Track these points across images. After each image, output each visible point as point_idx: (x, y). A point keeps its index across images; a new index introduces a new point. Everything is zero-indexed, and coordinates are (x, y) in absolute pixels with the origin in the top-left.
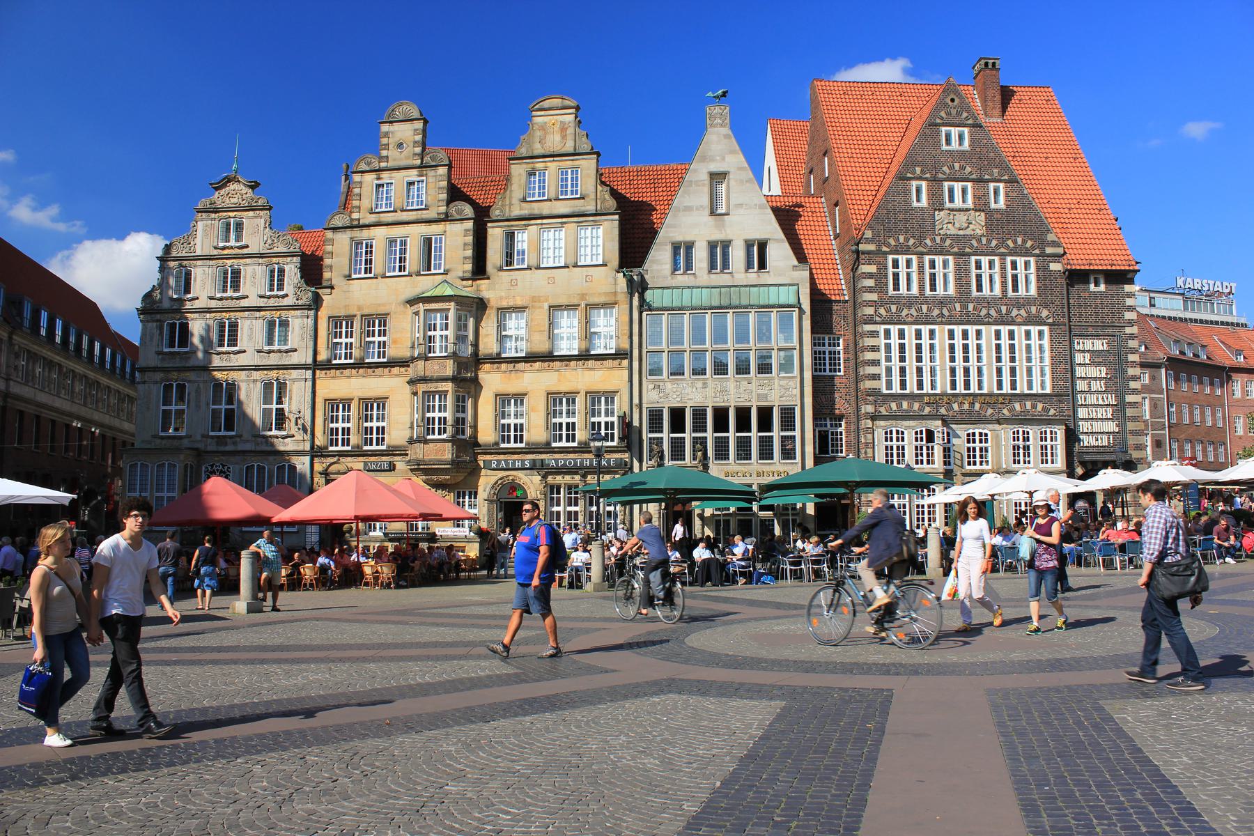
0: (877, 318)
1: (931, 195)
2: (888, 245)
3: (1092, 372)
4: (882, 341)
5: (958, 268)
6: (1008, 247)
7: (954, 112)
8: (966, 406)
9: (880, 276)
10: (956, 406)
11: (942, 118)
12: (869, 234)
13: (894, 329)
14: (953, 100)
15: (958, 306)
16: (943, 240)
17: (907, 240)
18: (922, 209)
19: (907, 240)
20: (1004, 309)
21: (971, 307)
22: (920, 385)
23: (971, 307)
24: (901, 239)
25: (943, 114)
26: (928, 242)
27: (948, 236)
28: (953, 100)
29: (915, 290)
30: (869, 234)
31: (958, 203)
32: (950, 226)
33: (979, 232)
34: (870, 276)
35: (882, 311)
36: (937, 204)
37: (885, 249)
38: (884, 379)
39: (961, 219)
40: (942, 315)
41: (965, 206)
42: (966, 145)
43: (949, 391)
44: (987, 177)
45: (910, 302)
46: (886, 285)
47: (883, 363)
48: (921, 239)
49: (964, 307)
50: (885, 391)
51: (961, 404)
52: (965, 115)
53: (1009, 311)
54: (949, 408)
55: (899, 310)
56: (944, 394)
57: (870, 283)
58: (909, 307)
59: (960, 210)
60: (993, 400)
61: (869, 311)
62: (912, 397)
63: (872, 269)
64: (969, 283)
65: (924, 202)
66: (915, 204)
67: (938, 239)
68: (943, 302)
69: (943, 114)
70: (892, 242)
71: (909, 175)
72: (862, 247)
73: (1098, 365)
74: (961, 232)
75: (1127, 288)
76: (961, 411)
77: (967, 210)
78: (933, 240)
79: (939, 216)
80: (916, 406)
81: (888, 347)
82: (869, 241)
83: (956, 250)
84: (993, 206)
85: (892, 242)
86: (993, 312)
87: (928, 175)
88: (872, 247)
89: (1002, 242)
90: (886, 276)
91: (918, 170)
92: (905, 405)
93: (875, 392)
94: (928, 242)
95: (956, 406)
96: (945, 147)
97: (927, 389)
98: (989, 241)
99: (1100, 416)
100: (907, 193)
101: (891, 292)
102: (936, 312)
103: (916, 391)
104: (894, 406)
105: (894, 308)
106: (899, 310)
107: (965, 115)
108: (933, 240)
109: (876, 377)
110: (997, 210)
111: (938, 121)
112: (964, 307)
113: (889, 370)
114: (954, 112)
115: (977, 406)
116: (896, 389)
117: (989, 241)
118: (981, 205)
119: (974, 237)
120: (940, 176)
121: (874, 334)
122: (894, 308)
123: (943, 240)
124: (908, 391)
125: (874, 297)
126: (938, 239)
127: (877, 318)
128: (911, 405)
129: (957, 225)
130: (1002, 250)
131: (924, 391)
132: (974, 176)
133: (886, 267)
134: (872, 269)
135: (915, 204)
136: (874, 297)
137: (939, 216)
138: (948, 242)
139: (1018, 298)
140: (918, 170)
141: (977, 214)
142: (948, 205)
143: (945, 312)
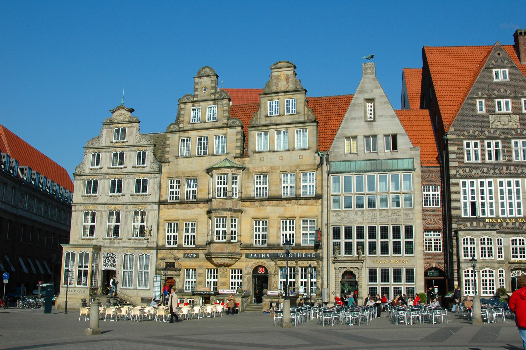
0: (458, 176)
2: (464, 135)
8: (511, 224)
9: (460, 153)
13: (468, 181)
15: (504, 168)
17: (474, 132)
19: (474, 132)
21: (512, 168)
23: (512, 168)
24: (471, 131)
26: (486, 133)
27: (498, 129)
33: (516, 126)
34: (454, 152)
35: (461, 172)
36: (491, 111)
37: (462, 137)
38: (463, 209)
39: (505, 119)
40: (495, 173)
41: (508, 112)
44: (520, 95)
45: (476, 166)
46: (463, 157)
47: (462, 201)
48: (482, 132)
49: (508, 168)
50: (463, 216)
51: (507, 223)
54: (501, 225)
55: (471, 171)
58: (476, 170)
59: (504, 114)
65: (484, 111)
66: (479, 112)
67: (492, 131)
68: (494, 166)
70: (466, 134)
74: (505, 127)
76: (508, 227)
77: (508, 114)
78: (489, 132)
79: (491, 118)
80: (481, 224)
81: (465, 192)
82: (452, 133)
83: (502, 137)
85: (466, 134)
87: (486, 96)
88: (454, 137)
90: (463, 152)
92: (475, 224)
93: (459, 216)
94: (486, 133)
101: (466, 161)
102: (492, 172)
104: (468, 224)
106: (471, 171)
108: (489, 132)
109: (458, 208)
112: (508, 168)
113: (465, 204)
119: (513, 129)
120: (493, 96)
121: (457, 185)
126: (492, 131)
127: (458, 176)
129: (502, 123)
132: (512, 95)
133: (463, 148)
135: (479, 112)
136: (456, 164)
137: (491, 118)
138: (498, 132)
141: (514, 116)
143: (497, 171)
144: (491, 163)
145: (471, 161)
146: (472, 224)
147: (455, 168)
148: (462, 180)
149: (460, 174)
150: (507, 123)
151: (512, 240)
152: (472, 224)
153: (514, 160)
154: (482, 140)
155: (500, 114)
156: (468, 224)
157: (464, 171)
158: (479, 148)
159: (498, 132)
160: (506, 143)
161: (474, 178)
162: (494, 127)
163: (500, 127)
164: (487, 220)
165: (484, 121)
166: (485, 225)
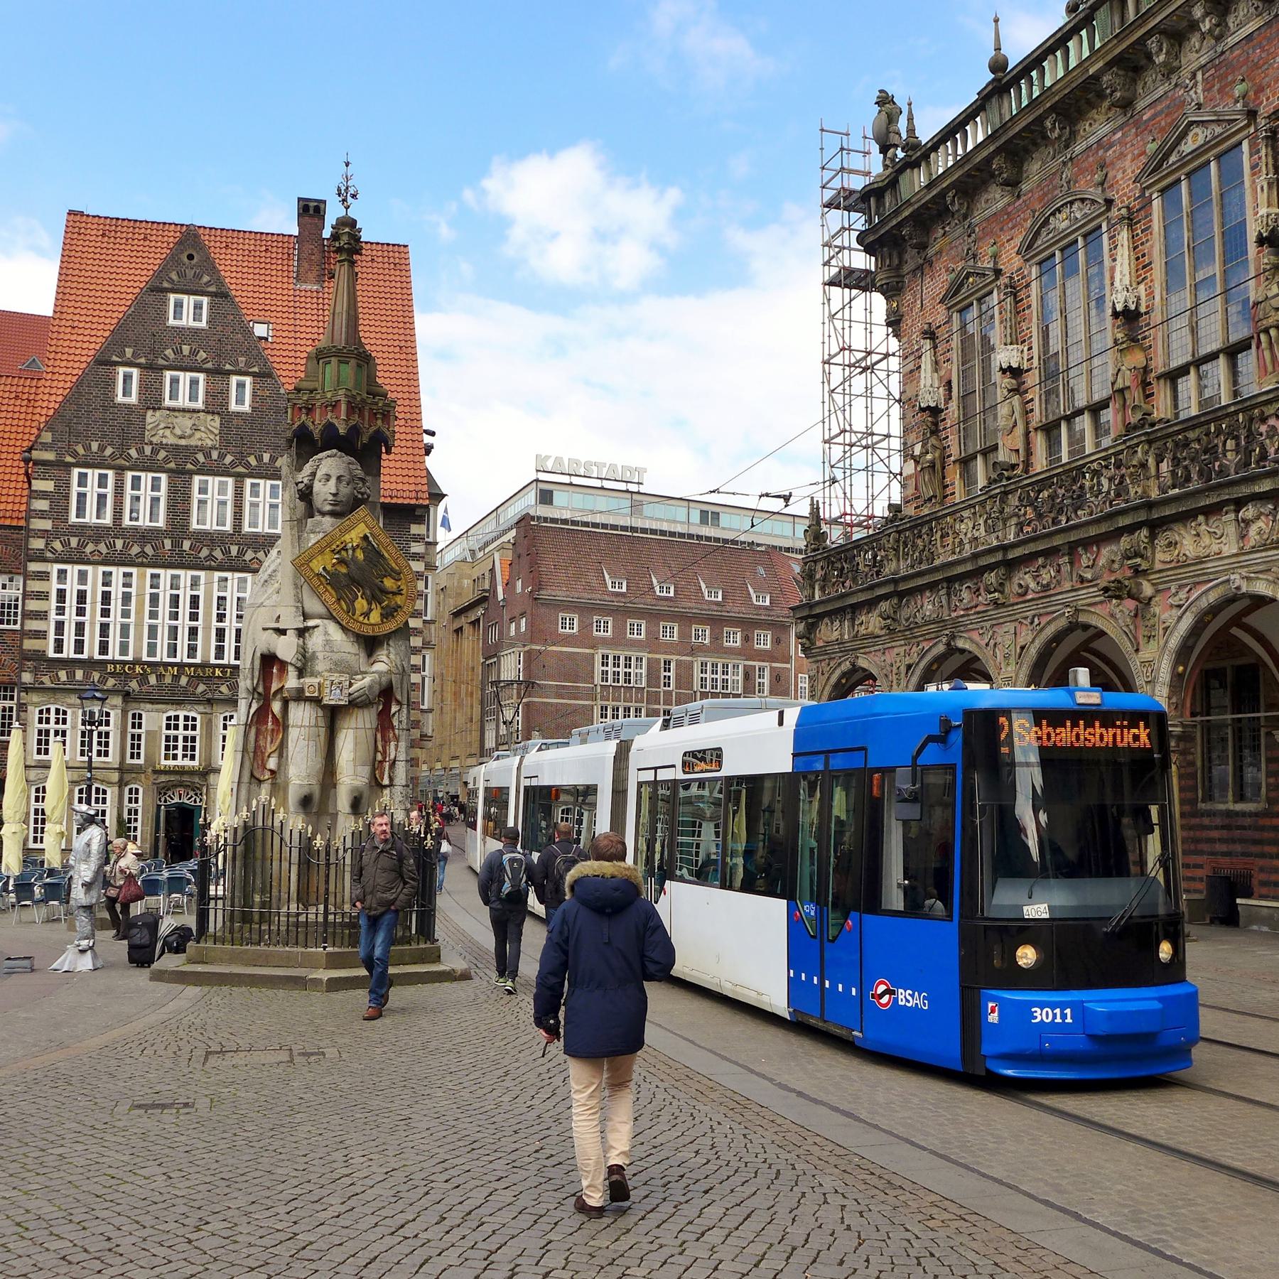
0: (49, 555)
2: (75, 454)
4: (54, 586)
5: (172, 491)
6: (248, 465)
8: (168, 680)
9: (59, 499)
10: (153, 680)
12: (47, 437)
13: (73, 570)
15: (168, 543)
16: (155, 452)
17: (102, 448)
18: (128, 407)
19: (102, 448)
20: (234, 550)
21: (186, 545)
22: (104, 648)
23: (186, 545)
24: (95, 446)
26: (133, 452)
27: (162, 446)
29: (107, 520)
30: (47, 437)
31: (183, 401)
32: (168, 432)
33: (210, 443)
34: (43, 495)
35: (57, 545)
36: (152, 400)
37: (69, 459)
38: (52, 636)
39: (185, 423)
40: (143, 554)
41: (193, 405)
42: (203, 324)
43: (145, 658)
44: (228, 367)
45: (98, 534)
47: (53, 616)
49: (177, 544)
50: (51, 654)
51: (160, 677)
52: (206, 278)
53: (241, 553)
54: (143, 679)
55: (82, 545)
56: (137, 662)
58: (97, 543)
59: (184, 410)
60: (208, 671)
61: (38, 544)
62: (90, 664)
63: (48, 486)
64: (187, 512)
65: (133, 399)
66: (120, 398)
67: (148, 450)
69: (174, 276)
71: (115, 358)
72: (36, 455)
74: (183, 442)
75: (415, 529)
76: (159, 686)
77: (194, 411)
80: (96, 676)
81: (61, 595)
82: (46, 447)
83: (172, 465)
84: (233, 407)
86: (218, 554)
87: (143, 360)
88: (50, 456)
89: (241, 459)
90: (67, 497)
92: (79, 675)
93: (40, 656)
94: (133, 452)
95: (153, 680)
96: (172, 322)
97: (114, 653)
98: (221, 456)
100: (111, 383)
101: (73, 518)
102: (135, 550)
103: (97, 657)
104: (63, 675)
105: (74, 542)
106: (82, 545)
109: (41, 635)
110: (238, 414)
111: (166, 285)
112: (177, 544)
113: (60, 626)
115: (184, 680)
116: (69, 652)
117: (221, 456)
118: (216, 403)
119: (201, 449)
120: (161, 362)
121: (44, 576)
122: (74, 542)
123: (155, 452)
124: (85, 656)
125: (47, 525)
126: (148, 450)
127: (49, 555)
128: (87, 676)
129: (178, 432)
130: (241, 469)
131: (109, 657)
132: (209, 365)
133: (68, 486)
134: (48, 486)
135: (120, 398)
136: (47, 525)
138: (162, 454)
139: (256, 535)
141: (210, 417)
142: (167, 402)
144: (136, 529)
145: (87, 520)
146: (71, 675)
147: (44, 534)
148: (57, 567)
149: (54, 551)
150: (189, 432)
151: (169, 718)
152: (71, 675)
153: (194, 526)
154: (120, 470)
155: (174, 410)
156: (63, 675)
157: (66, 544)
158: (109, 490)
159: (162, 454)
160: (179, 481)
161: (88, 563)
162: (155, 440)
163: (171, 440)
164: (110, 668)
165: (130, 423)
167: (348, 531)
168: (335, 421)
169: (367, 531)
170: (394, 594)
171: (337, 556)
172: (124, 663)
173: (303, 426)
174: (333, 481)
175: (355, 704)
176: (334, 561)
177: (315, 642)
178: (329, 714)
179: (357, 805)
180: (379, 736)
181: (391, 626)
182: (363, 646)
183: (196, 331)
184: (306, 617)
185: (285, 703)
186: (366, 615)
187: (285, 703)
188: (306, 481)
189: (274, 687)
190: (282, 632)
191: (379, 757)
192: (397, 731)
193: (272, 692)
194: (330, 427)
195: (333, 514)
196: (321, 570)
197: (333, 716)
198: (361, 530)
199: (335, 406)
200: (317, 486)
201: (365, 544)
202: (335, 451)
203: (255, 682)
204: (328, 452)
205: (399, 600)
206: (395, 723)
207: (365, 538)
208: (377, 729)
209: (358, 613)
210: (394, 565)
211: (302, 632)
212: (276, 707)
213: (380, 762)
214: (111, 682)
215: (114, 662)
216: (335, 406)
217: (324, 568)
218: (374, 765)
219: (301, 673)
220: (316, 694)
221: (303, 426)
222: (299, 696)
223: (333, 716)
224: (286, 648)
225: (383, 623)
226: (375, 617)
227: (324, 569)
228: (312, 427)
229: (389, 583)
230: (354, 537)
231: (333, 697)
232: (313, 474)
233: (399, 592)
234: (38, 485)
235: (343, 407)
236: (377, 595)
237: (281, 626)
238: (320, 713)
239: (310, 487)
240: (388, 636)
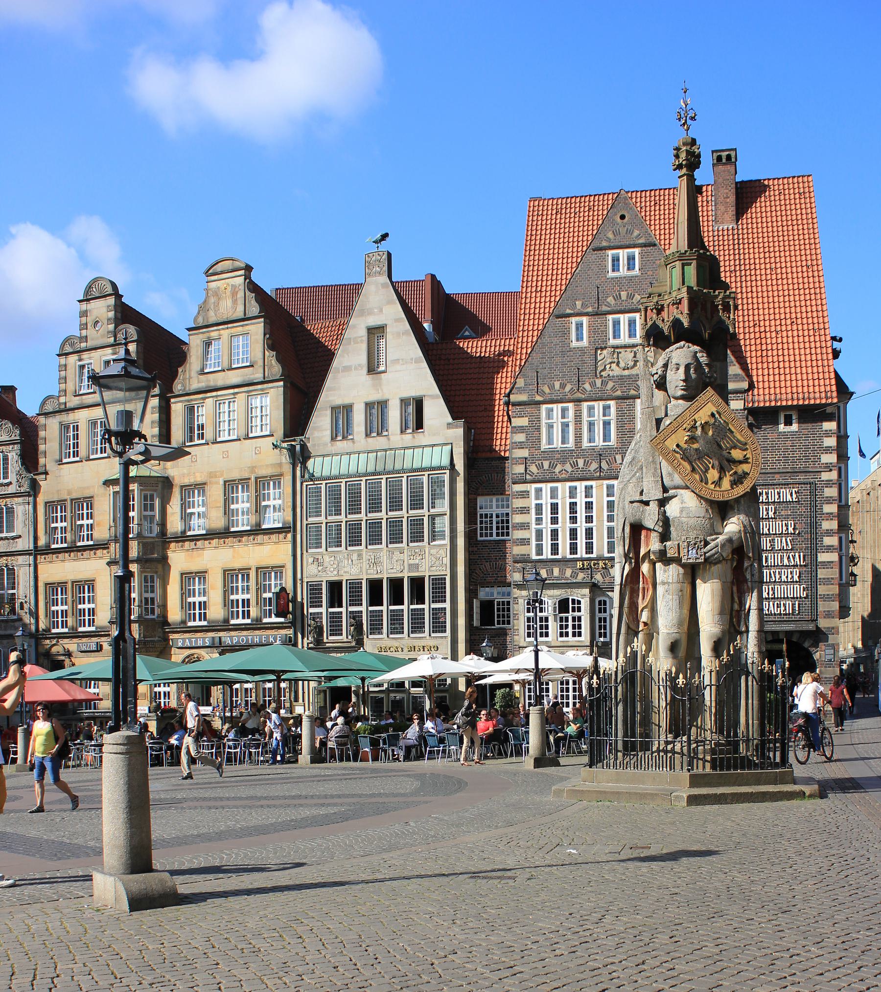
1: (592, 330)
3: (777, 526)
4: (533, 502)
5: (620, 413)
7: (623, 231)
11: (609, 240)
13: (546, 487)
14: (623, 217)
17: (563, 386)
18: (582, 350)
19: (563, 386)
22: (574, 549)
24: (557, 385)
25: (610, 235)
26: (587, 386)
28: (623, 217)
29: (571, 444)
31: (624, 338)
35: (533, 469)
38: (534, 542)
41: (633, 341)
42: (636, 271)
45: (564, 456)
46: (539, 439)
47: (534, 526)
50: (534, 557)
55: (552, 466)
56: (600, 558)
57: (521, 437)
58: (564, 463)
59: (625, 347)
62: (564, 561)
63: (523, 422)
65: (585, 342)
66: (574, 344)
67: (598, 382)
70: (547, 390)
71: (568, 311)
72: (513, 398)
73: (787, 518)
74: (626, 373)
77: (634, 346)
78: (593, 385)
80: (568, 572)
81: (539, 508)
82: (521, 391)
83: (619, 393)
85: (547, 390)
87: (590, 310)
88: (523, 398)
90: (539, 429)
91: (579, 304)
94: (587, 386)
99: (784, 578)
100: (566, 333)
101: (544, 445)
102: (594, 466)
103: (569, 556)
106: (552, 466)
107: (636, 233)
109: (525, 542)
111: (604, 244)
113: (539, 534)
114: (623, 231)
116: (547, 554)
121: (525, 495)
122: (546, 465)
124: (559, 557)
126: (598, 382)
128: (562, 572)
131: (578, 556)
133: (539, 419)
134: (523, 422)
135: (574, 344)
136: (525, 453)
138: (610, 384)
140: (579, 304)
144: (593, 449)
148: (534, 486)
149: (532, 474)
157: (540, 467)
159: (610, 384)
166: (574, 575)
167: (698, 410)
168: (679, 316)
169: (714, 410)
170: (740, 462)
171: (688, 434)
172: (590, 559)
173: (654, 325)
174: (682, 370)
175: (708, 561)
176: (686, 438)
177: (672, 509)
178: (689, 571)
179: (717, 649)
180: (735, 589)
181: (740, 490)
182: (717, 510)
183: (631, 279)
184: (665, 490)
185: (653, 564)
186: (718, 483)
187: (653, 564)
188: (660, 372)
189: (642, 552)
190: (647, 503)
191: (736, 607)
192: (749, 584)
193: (641, 556)
194: (677, 323)
195: (682, 397)
196: (675, 447)
197: (693, 572)
198: (710, 408)
199: (678, 303)
200: (670, 375)
201: (712, 421)
202: (682, 343)
203: (626, 548)
204: (678, 345)
205: (745, 467)
206: (748, 576)
207: (713, 415)
208: (732, 583)
209: (710, 482)
210: (739, 437)
211: (662, 503)
212: (645, 568)
213: (737, 611)
214: (581, 576)
215: (582, 560)
216: (678, 303)
217: (678, 446)
218: (731, 615)
219: (665, 537)
220: (676, 555)
221: (654, 325)
222: (664, 558)
223: (693, 572)
224: (650, 517)
225: (733, 488)
226: (726, 483)
227: (678, 446)
228: (661, 325)
229: (737, 454)
230: (703, 416)
231: (691, 556)
232: (666, 366)
233: (745, 461)
234: (516, 422)
235: (685, 303)
236: (726, 464)
237: (644, 498)
238: (681, 570)
239: (663, 377)
240: (737, 500)
